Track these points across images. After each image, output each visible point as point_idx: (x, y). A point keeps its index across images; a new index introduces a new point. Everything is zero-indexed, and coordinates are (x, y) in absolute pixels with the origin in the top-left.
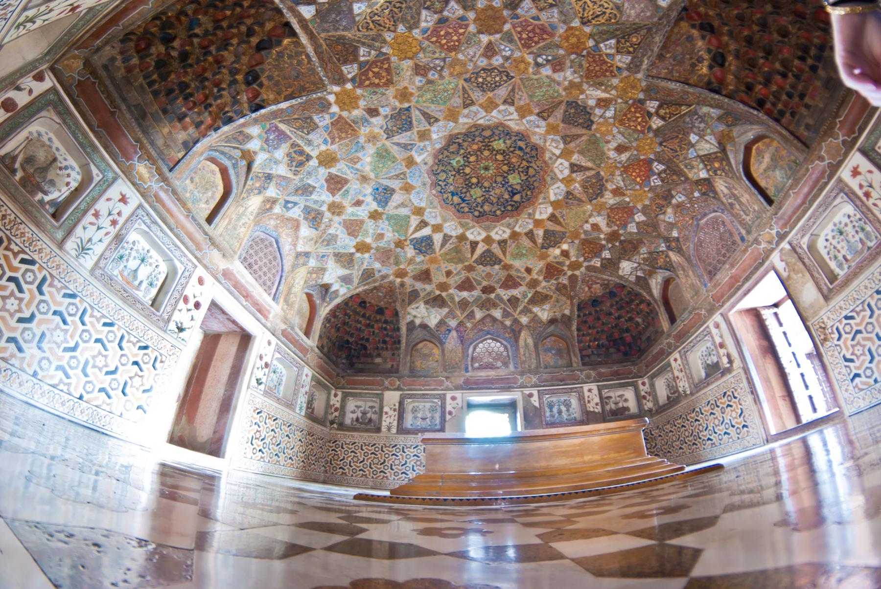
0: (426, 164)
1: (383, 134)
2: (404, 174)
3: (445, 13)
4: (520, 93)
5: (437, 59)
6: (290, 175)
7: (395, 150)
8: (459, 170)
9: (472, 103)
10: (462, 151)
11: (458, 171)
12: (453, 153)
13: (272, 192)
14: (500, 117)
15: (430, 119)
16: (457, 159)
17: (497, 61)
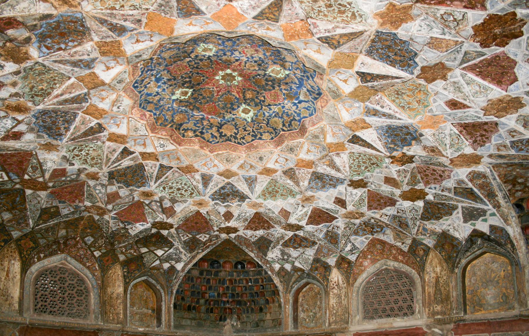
0: (261, 159)
1: (246, 202)
2: (285, 173)
3: (122, 225)
4: (110, 156)
5: (153, 210)
6: (316, 247)
7: (259, 188)
8: (256, 105)
9: (161, 166)
10: (228, 116)
11: (259, 104)
12: (236, 125)
13: (332, 261)
14: (148, 142)
15: (206, 180)
16: (243, 115)
17: (112, 189)
